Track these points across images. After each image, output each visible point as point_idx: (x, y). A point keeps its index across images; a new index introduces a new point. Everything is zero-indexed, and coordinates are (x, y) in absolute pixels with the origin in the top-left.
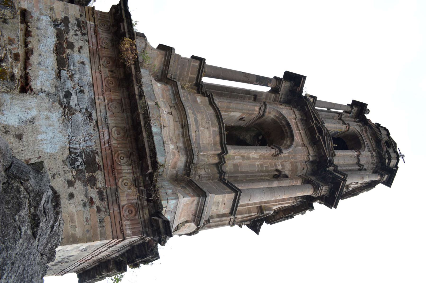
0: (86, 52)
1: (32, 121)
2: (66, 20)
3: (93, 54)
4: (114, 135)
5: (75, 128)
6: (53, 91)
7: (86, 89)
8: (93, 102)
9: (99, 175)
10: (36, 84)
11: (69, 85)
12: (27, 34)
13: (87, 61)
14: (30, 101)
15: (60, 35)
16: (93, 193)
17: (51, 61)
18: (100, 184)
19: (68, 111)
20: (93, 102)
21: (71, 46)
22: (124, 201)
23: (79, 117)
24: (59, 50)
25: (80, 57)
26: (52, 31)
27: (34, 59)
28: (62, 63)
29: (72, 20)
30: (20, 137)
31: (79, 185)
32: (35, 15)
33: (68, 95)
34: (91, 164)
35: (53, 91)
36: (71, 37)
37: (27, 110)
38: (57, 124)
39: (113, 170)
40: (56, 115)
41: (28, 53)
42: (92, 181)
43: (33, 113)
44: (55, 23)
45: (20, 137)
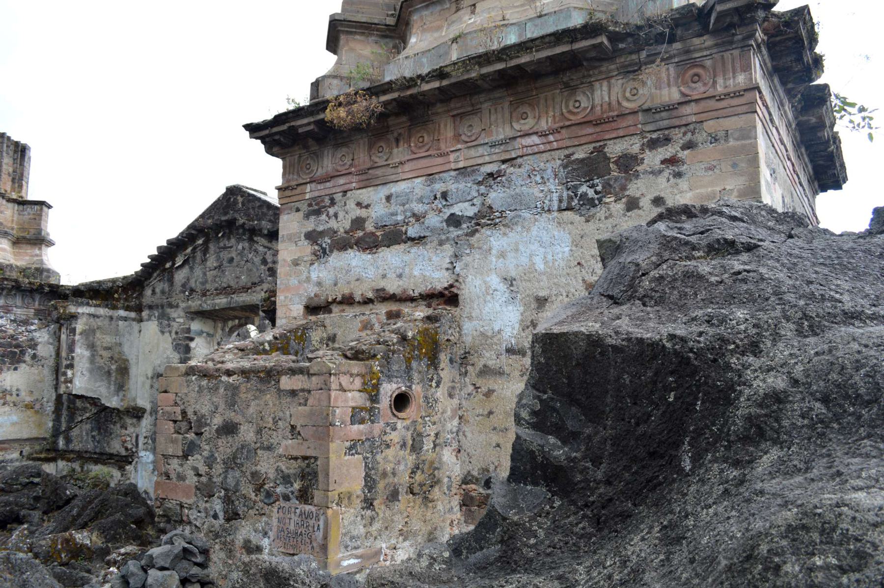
0: (365, 195)
1: (510, 282)
2: (312, 237)
3: (368, 180)
4: (528, 124)
5: (519, 203)
6: (448, 250)
7: (439, 187)
8: (462, 172)
9: (615, 149)
10: (440, 280)
11: (434, 220)
12: (348, 301)
13: (383, 191)
14: (471, 287)
15: (343, 245)
16: (653, 159)
17: (392, 257)
18: (634, 146)
19: (487, 218)
20: (462, 172)
21: (359, 223)
22: (671, 94)
24: (370, 244)
25: (377, 205)
26: (337, 260)
27: (393, 286)
28: (393, 236)
29: (311, 225)
30: (542, 302)
31: (635, 188)
32: (312, 290)
33: (454, 221)
34: (592, 167)
35: (448, 250)
36: (342, 224)
37: (489, 291)
38: (513, 236)
39: (604, 122)
40: (496, 240)
41: (384, 297)
42: (628, 163)
43: (494, 281)
44: (321, 254)
45: (542, 302)
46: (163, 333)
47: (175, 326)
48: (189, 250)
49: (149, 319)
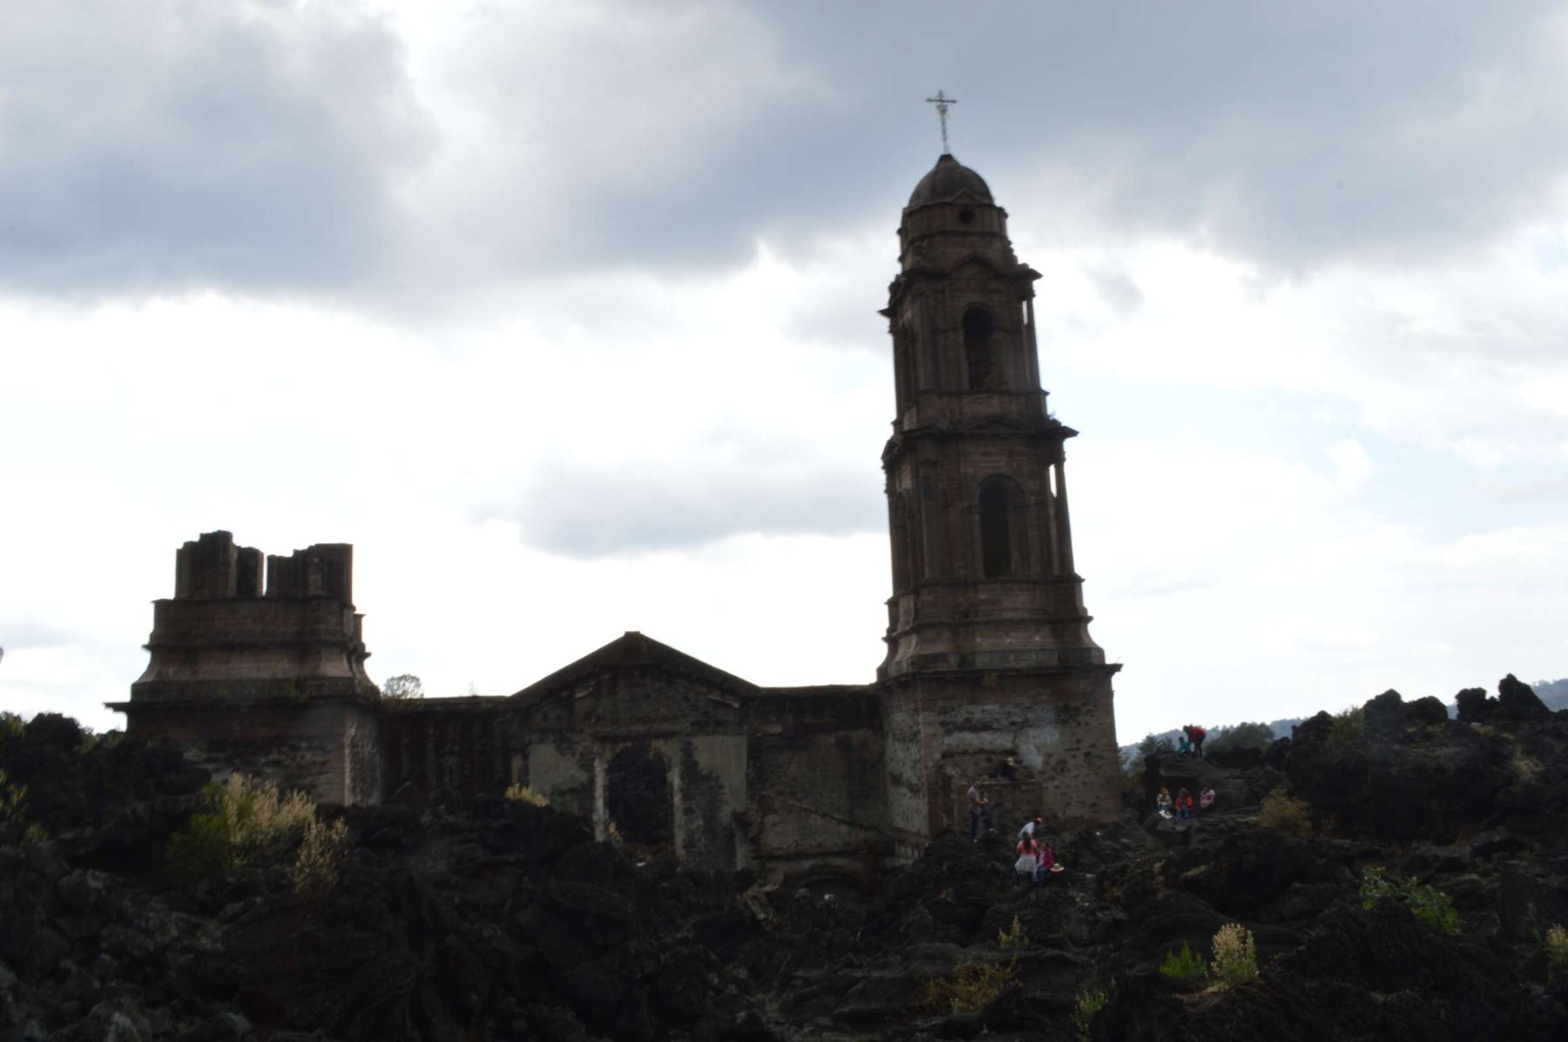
0: (971, 708)
1: (1037, 747)
2: (943, 724)
3: (973, 702)
9: (1073, 704)
10: (1009, 745)
11: (1005, 723)
12: (965, 753)
14: (1023, 748)
15: (961, 728)
16: (1084, 709)
18: (1079, 704)
20: (1017, 705)
21: (968, 720)
23: (1030, 715)
25: (977, 713)
27: (988, 747)
28: (986, 727)
29: (941, 718)
30: (1050, 755)
31: (1079, 718)
33: (1013, 723)
36: (960, 719)
40: (1032, 732)
41: (982, 751)
42: (1077, 709)
44: (949, 732)
46: (563, 754)
47: (580, 748)
48: (592, 683)
49: (542, 741)
